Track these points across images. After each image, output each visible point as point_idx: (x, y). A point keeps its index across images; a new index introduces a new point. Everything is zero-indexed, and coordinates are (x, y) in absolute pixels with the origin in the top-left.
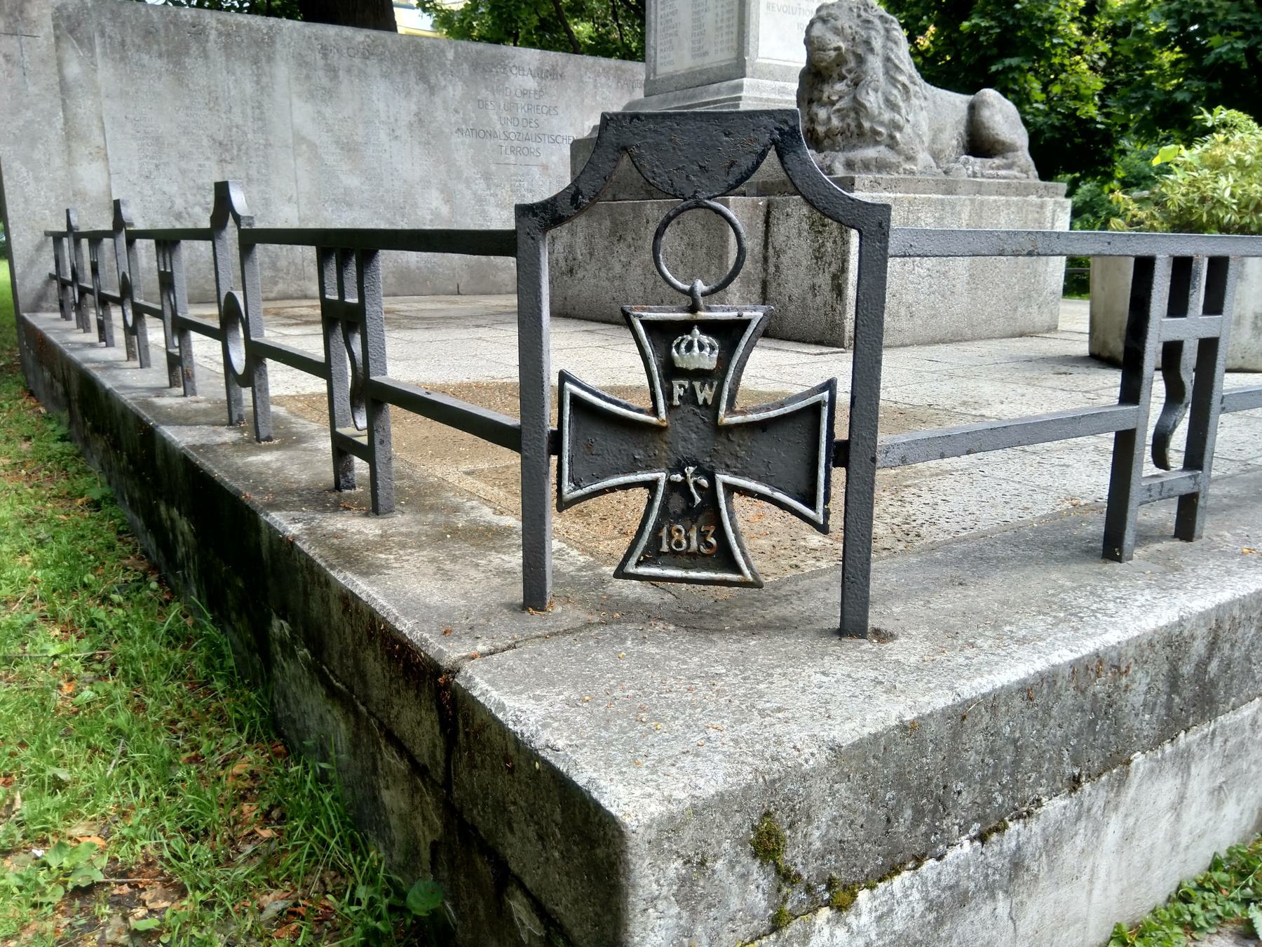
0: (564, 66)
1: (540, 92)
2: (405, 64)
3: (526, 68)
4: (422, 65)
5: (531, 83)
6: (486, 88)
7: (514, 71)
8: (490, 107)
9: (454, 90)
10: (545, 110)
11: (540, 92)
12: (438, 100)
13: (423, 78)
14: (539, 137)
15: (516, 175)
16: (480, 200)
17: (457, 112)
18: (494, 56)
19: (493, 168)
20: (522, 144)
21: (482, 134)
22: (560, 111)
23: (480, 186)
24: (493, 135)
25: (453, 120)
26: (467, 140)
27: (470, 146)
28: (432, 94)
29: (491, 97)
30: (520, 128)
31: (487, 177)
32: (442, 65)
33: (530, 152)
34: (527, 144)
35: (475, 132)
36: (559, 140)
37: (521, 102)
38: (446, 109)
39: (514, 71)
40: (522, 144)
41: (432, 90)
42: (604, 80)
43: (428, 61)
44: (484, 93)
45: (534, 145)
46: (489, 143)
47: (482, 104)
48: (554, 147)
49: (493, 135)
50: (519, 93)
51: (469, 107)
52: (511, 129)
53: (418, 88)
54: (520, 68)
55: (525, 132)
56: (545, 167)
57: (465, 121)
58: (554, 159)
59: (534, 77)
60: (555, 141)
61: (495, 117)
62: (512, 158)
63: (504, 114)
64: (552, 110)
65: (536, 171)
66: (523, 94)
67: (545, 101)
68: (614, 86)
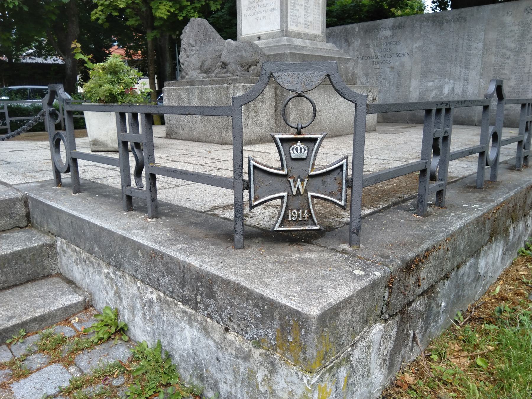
2: (341, 37)
3: (387, 27)
4: (346, 36)
5: (388, 33)
6: (370, 39)
7: (382, 30)
8: (371, 46)
9: (357, 43)
10: (394, 43)
11: (392, 37)
12: (351, 48)
13: (346, 40)
14: (390, 55)
15: (379, 73)
17: (357, 51)
19: (370, 71)
22: (401, 42)
24: (371, 57)
25: (356, 54)
27: (361, 64)
28: (349, 46)
29: (371, 42)
30: (382, 53)
31: (367, 75)
32: (353, 34)
33: (386, 62)
34: (385, 59)
35: (364, 58)
36: (400, 55)
38: (354, 51)
41: (349, 44)
42: (425, 23)
43: (349, 34)
44: (369, 41)
45: (388, 59)
47: (367, 46)
49: (371, 57)
50: (383, 38)
51: (362, 48)
52: (378, 54)
53: (344, 45)
54: (384, 28)
55: (384, 54)
56: (392, 68)
57: (360, 54)
58: (397, 64)
59: (390, 30)
60: (398, 56)
62: (378, 66)
64: (397, 43)
65: (388, 70)
66: (385, 38)
67: (395, 39)
68: (431, 25)
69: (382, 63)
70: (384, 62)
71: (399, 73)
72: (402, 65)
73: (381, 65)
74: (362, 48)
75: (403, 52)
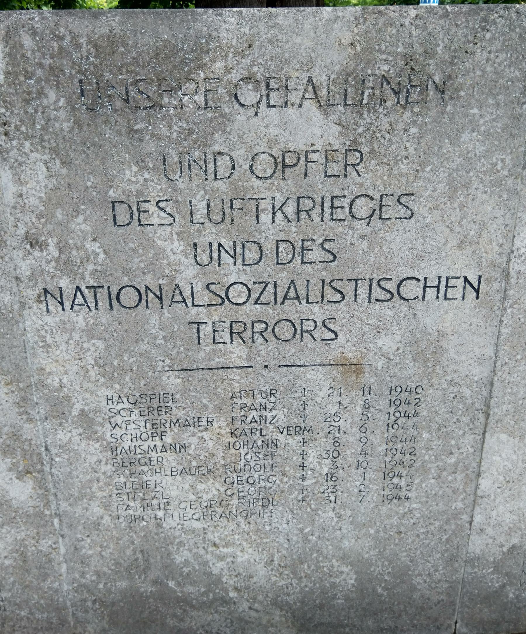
0: (459, 53)
1: (350, 157)
3: (297, 77)
5: (312, 128)
6: (141, 162)
7: (249, 96)
8: (156, 217)
10: (363, 207)
11: (350, 157)
14: (333, 290)
15: (243, 393)
16: (129, 463)
17: (34, 242)
18: (165, 53)
19: (173, 382)
20: (271, 313)
21: (129, 297)
23: (131, 429)
24: (168, 295)
26: (80, 318)
27: (90, 333)
29: (157, 189)
31: (153, 405)
33: (298, 330)
34: (289, 310)
36: (411, 290)
37: (271, 192)
39: (249, 96)
40: (271, 313)
44: (130, 178)
45: (318, 312)
46: (154, 319)
48: (387, 311)
50: (263, 165)
52: (232, 272)
54: (271, 87)
55: (283, 278)
56: (352, 368)
57: (66, 266)
58: (387, 343)
59: (325, 106)
60: (396, 294)
61: (178, 246)
62: (238, 353)
63: (210, 234)
64: (391, 206)
65: (319, 383)
66: (281, 166)
67: (371, 178)
69: (269, 331)
70: (284, 330)
71: (404, 401)
72: (428, 352)
73: (266, 350)
74: (80, 224)
75: (430, 271)
